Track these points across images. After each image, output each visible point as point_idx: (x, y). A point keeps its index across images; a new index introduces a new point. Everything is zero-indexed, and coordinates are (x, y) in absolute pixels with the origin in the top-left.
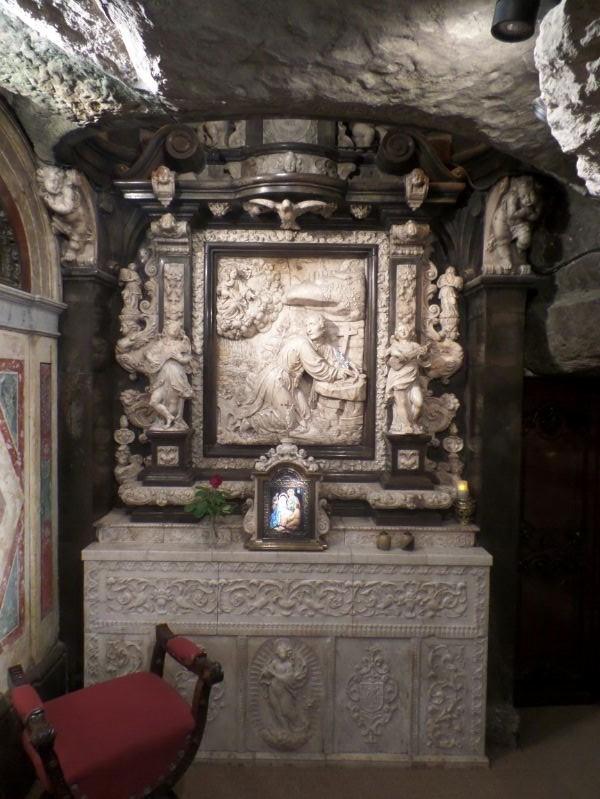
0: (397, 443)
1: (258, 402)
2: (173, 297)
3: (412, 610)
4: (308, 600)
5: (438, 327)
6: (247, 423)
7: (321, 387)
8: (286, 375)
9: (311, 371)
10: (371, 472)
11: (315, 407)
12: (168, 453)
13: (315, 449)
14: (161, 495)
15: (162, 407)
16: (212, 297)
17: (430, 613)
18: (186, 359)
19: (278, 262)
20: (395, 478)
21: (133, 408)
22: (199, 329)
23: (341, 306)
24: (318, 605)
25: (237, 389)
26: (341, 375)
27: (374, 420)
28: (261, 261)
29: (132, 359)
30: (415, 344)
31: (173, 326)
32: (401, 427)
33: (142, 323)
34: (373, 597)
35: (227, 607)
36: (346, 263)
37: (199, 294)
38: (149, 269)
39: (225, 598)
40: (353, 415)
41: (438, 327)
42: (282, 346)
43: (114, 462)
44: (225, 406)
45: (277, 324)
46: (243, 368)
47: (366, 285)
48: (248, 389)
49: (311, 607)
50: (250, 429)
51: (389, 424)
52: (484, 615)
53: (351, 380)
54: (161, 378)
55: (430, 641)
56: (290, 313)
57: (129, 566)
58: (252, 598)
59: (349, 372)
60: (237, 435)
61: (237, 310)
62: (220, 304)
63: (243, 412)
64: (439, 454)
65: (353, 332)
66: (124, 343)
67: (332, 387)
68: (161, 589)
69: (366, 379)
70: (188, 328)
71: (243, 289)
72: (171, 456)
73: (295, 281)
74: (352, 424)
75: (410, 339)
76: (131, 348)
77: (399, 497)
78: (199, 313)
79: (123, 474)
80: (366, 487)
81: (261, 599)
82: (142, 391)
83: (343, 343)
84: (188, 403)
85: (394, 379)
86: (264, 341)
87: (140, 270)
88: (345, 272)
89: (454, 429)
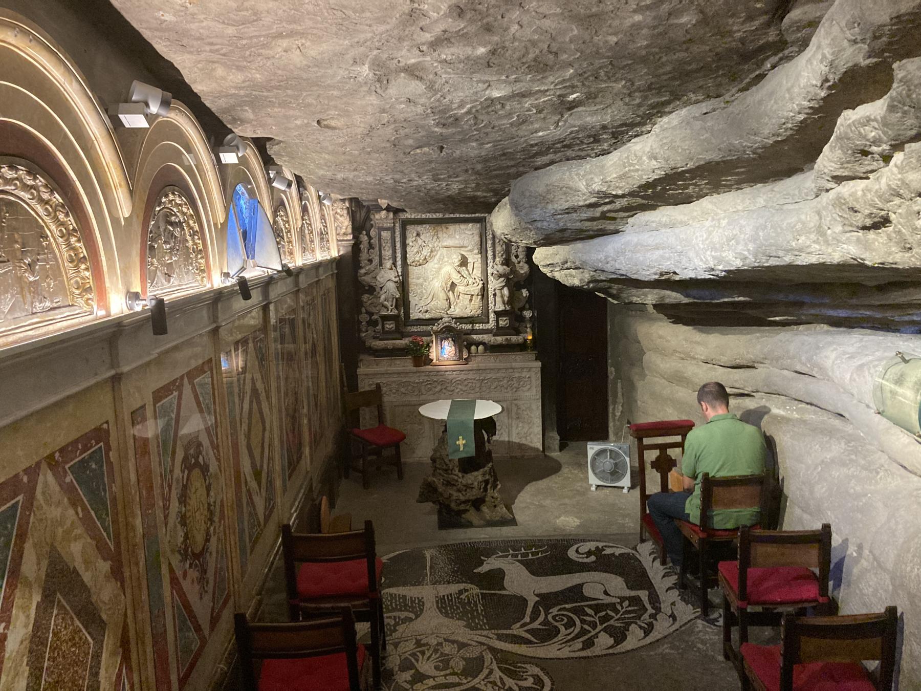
0: (498, 314)
1: (431, 297)
2: (387, 248)
3: (507, 389)
4: (460, 387)
5: (517, 257)
6: (425, 308)
7: (460, 288)
8: (444, 284)
9: (455, 282)
10: (488, 329)
11: (458, 299)
12: (390, 325)
13: (461, 320)
14: (390, 344)
15: (386, 303)
16: (404, 246)
17: (515, 390)
18: (397, 279)
19: (439, 228)
20: (499, 331)
21: (368, 303)
22: (399, 262)
23: (469, 248)
24: (464, 389)
25: (419, 291)
26: (471, 281)
27: (488, 304)
28: (428, 226)
29: (367, 279)
30: (505, 267)
31: (388, 264)
32: (500, 307)
33: (370, 261)
34: (489, 384)
35: (423, 391)
36: (470, 225)
37: (398, 245)
38: (373, 233)
39: (423, 387)
40: (477, 301)
41: (517, 257)
42: (440, 269)
43: (360, 331)
44: (413, 300)
45: (437, 257)
46: (421, 280)
47: (481, 237)
48: (424, 291)
49: (461, 390)
50: (427, 311)
51: (495, 305)
52: (539, 389)
53: (476, 284)
54: (384, 289)
55: (516, 402)
56: (444, 251)
57: (379, 376)
58: (435, 387)
59: (474, 281)
60: (420, 314)
61: (418, 252)
62: (408, 249)
63: (422, 303)
64: (521, 319)
65: (476, 260)
66: (363, 271)
67: (467, 289)
68: (394, 385)
69: (483, 284)
70: (394, 264)
71: (420, 242)
72: (392, 326)
73: (445, 235)
74: (477, 306)
75: (502, 264)
76: (366, 274)
77: (500, 339)
78: (399, 255)
79: (365, 336)
80: (485, 336)
81: (439, 388)
82: (371, 294)
83: (470, 267)
84: (397, 299)
85: (494, 284)
86: (432, 265)
87: (368, 235)
88: (470, 230)
89: (527, 306)
